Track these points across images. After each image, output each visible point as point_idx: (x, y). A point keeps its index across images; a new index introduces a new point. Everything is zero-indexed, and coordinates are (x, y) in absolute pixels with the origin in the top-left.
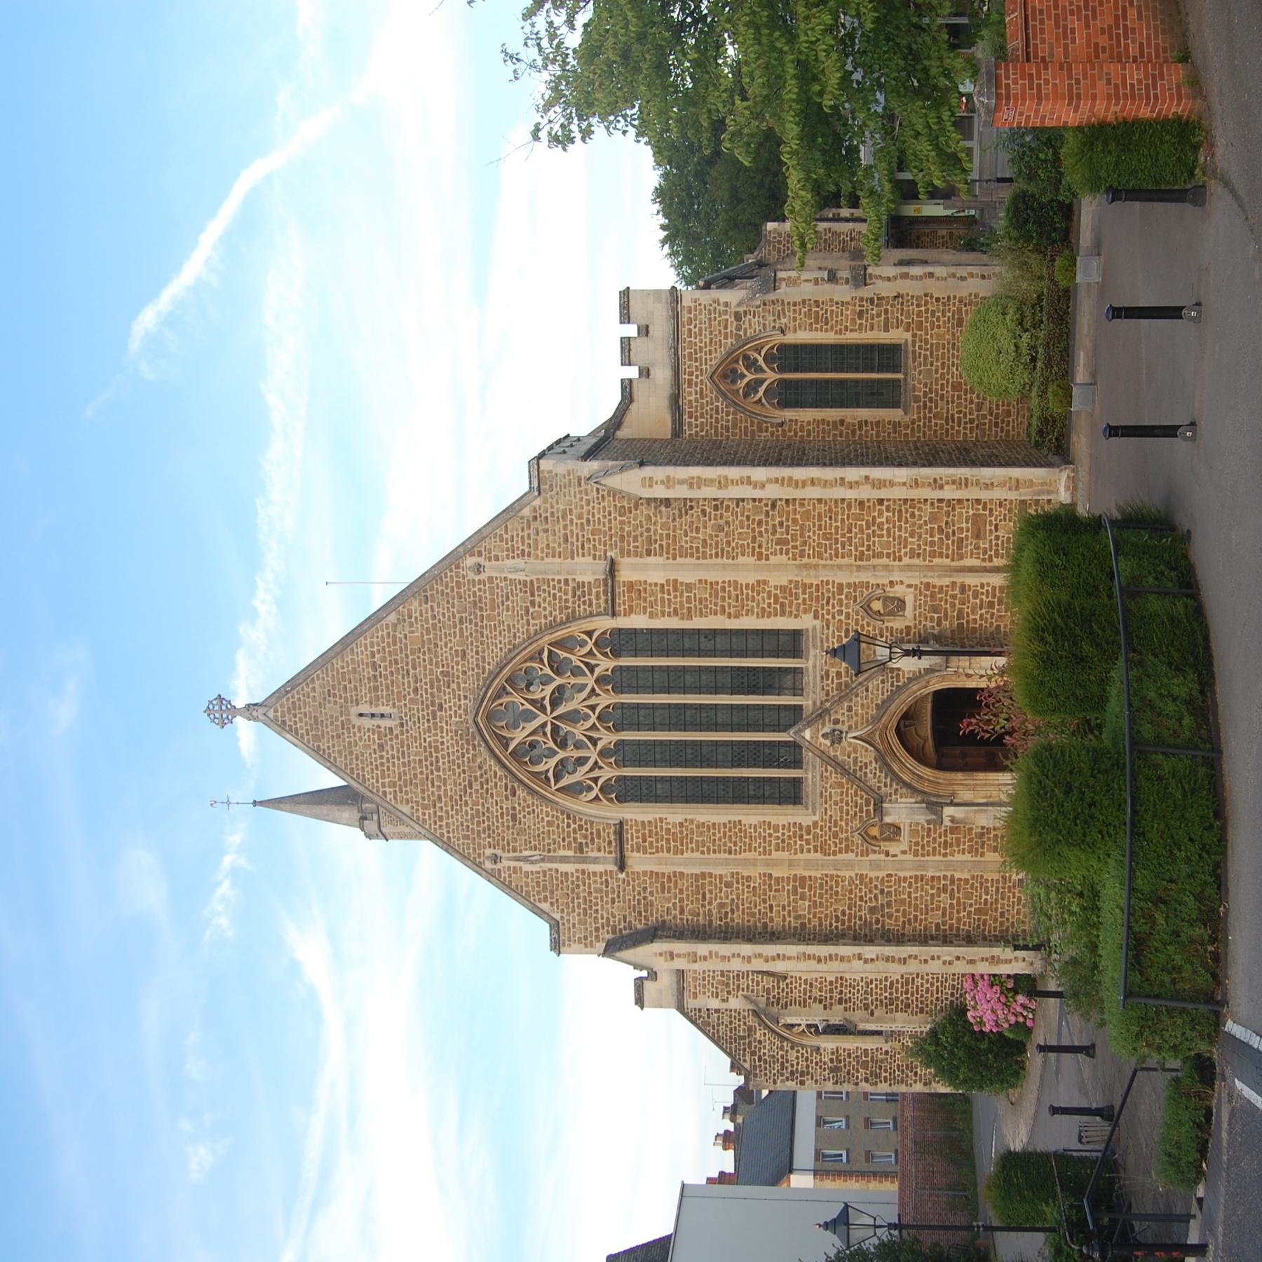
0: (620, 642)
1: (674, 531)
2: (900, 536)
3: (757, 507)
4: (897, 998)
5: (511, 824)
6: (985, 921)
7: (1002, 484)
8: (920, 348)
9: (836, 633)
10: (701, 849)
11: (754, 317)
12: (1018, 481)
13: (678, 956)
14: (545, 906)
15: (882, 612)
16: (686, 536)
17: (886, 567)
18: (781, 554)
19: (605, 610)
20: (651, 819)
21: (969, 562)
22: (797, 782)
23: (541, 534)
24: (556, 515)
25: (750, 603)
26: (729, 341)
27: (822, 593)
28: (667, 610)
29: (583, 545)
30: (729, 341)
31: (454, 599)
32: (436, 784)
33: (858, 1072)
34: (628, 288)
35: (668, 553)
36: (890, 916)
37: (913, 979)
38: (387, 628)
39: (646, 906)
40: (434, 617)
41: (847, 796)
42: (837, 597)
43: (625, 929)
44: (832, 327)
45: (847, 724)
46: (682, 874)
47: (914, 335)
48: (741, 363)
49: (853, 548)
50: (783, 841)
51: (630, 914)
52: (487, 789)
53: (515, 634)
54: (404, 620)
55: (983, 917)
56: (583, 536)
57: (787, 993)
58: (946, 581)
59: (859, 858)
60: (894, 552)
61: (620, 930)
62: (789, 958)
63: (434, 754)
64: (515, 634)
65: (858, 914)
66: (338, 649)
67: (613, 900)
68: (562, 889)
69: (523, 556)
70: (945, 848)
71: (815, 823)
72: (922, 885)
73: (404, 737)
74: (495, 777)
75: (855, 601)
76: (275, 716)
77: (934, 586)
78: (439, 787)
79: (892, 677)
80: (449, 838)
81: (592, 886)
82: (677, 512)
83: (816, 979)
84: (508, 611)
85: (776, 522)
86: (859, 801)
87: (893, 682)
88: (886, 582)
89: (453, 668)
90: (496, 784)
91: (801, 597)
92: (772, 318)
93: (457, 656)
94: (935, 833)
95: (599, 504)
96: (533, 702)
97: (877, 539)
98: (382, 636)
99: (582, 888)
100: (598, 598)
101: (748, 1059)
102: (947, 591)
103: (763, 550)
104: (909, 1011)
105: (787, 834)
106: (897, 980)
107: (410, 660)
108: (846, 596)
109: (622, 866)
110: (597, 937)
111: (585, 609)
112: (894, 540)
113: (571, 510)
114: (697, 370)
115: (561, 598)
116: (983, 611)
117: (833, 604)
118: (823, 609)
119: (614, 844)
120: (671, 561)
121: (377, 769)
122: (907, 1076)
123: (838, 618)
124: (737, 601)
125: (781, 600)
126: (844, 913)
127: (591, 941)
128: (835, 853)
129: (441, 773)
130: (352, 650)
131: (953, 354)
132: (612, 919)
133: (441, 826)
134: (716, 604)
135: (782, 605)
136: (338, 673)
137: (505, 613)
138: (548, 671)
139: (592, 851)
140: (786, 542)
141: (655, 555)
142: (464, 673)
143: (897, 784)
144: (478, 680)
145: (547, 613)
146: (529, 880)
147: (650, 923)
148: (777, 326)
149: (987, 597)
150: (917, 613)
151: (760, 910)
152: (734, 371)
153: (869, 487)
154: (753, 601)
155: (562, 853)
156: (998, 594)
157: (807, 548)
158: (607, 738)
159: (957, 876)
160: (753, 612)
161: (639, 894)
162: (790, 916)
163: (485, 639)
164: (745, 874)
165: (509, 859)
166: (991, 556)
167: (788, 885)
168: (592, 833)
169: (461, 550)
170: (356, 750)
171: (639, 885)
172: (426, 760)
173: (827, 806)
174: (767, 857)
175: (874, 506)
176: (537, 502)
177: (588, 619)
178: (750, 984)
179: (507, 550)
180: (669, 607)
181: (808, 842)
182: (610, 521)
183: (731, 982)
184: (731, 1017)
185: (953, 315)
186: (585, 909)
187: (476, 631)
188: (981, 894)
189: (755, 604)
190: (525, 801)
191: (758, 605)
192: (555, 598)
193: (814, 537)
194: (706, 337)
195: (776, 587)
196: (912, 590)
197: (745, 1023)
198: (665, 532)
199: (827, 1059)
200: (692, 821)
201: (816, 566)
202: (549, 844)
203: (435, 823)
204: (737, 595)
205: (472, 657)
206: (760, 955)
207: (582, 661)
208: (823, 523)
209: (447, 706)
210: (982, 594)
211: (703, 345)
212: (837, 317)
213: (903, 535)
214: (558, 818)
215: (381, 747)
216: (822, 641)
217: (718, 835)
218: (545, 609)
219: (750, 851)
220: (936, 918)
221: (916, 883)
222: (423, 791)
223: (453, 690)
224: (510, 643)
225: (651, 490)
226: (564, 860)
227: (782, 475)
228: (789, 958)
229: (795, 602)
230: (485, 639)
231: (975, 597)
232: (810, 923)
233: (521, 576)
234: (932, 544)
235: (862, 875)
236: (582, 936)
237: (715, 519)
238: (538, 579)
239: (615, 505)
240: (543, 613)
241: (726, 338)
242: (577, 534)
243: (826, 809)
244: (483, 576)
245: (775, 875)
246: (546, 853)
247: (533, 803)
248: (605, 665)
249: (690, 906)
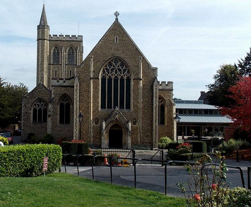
0: (129, 80)
13: (77, 88)
14: (83, 65)
21: (142, 134)
22: (105, 108)
58: (139, 131)
138: (124, 68)
140: (145, 107)
158: (113, 77)
234: (144, 129)
248: (125, 78)
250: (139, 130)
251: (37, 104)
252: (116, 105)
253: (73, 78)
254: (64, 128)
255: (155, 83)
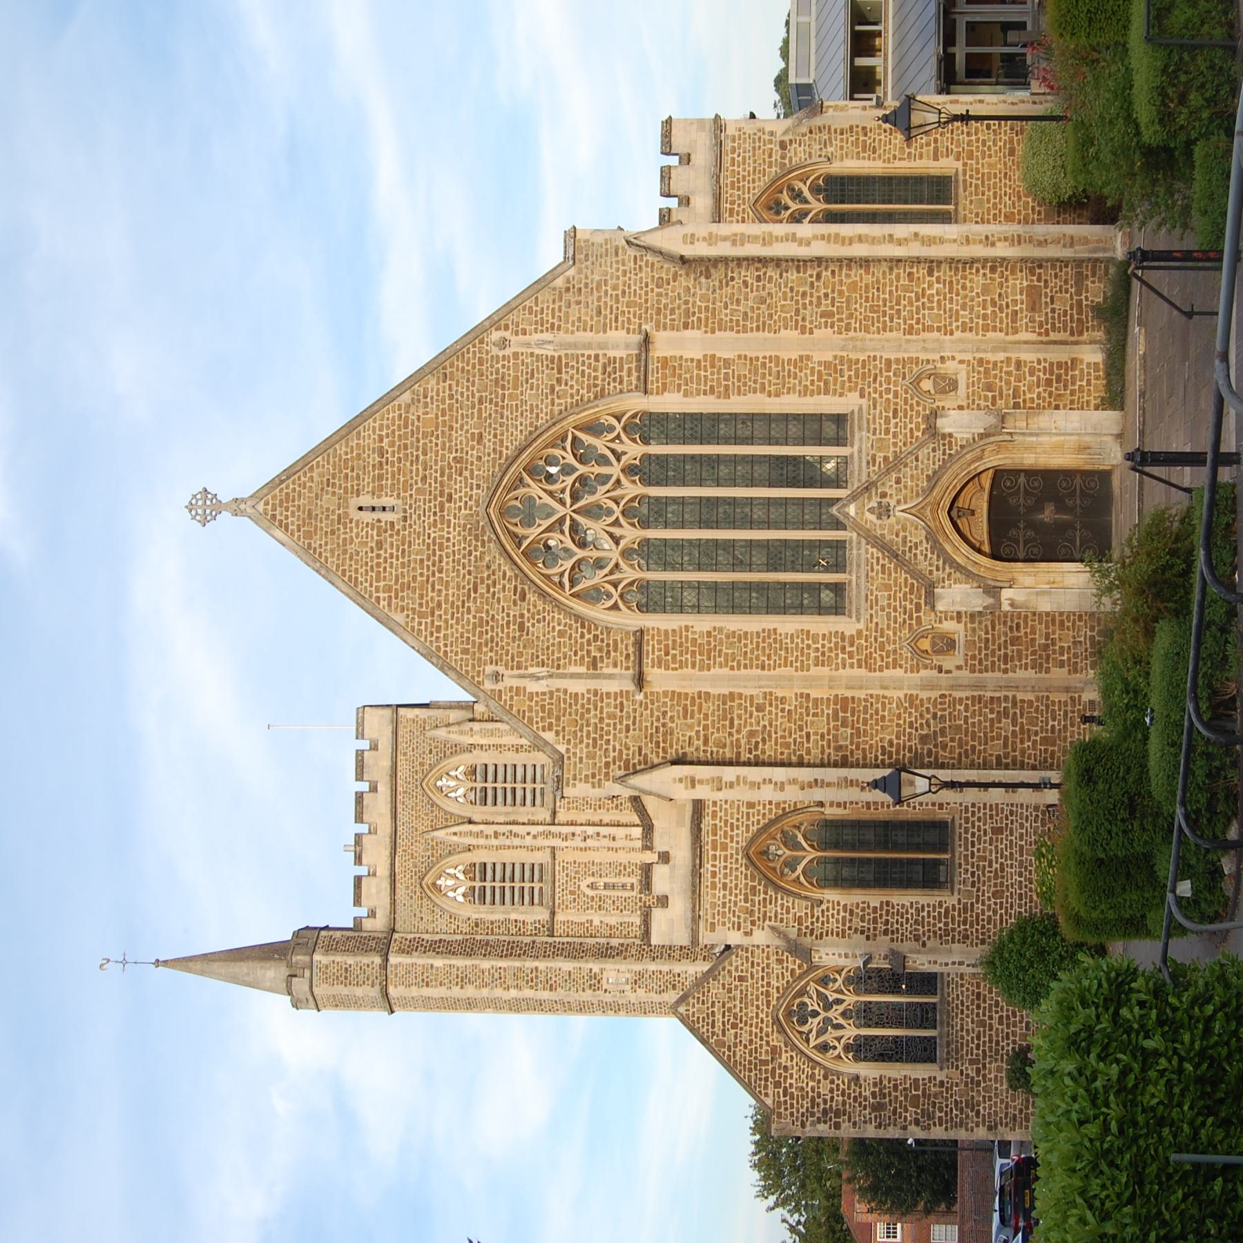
1: (714, 304)
2: (951, 309)
3: (801, 278)
4: (953, 930)
5: (517, 634)
6: (1053, 753)
7: (1056, 241)
8: (971, 177)
9: (884, 414)
10: (730, 664)
11: (800, 146)
12: (1072, 238)
13: (701, 782)
14: (549, 736)
15: (933, 392)
16: (726, 308)
17: (938, 340)
18: (826, 327)
19: (636, 387)
20: (676, 627)
21: (1024, 336)
22: (838, 589)
23: (573, 306)
24: (590, 286)
25: (791, 380)
26: (774, 169)
27: (869, 370)
28: (703, 388)
29: (617, 318)
30: (774, 169)
31: (474, 376)
32: (437, 587)
33: (906, 1111)
34: (670, 117)
35: (706, 326)
36: (944, 747)
37: (972, 904)
38: (399, 409)
39: (665, 734)
40: (451, 397)
41: (895, 601)
42: (885, 374)
43: (640, 764)
44: (880, 156)
45: (895, 498)
46: (707, 694)
47: (965, 164)
48: (785, 192)
49: (901, 321)
50: (823, 654)
51: (646, 745)
52: (494, 593)
53: (538, 414)
54: (419, 401)
55: (1050, 748)
56: (618, 308)
57: (823, 923)
58: (1001, 356)
59: (909, 674)
60: (945, 325)
61: (634, 764)
62: (829, 785)
63: (438, 553)
64: (538, 414)
65: (908, 744)
66: (343, 433)
67: (628, 726)
68: (570, 714)
69: (552, 328)
70: (1006, 663)
71: (859, 632)
72: (980, 708)
73: (407, 533)
74: (504, 579)
75: (904, 378)
76: (265, 509)
77: (988, 362)
78: (440, 591)
79: (944, 445)
80: (446, 652)
81: (605, 710)
82: (717, 284)
83: (858, 904)
84: (532, 389)
85: (821, 294)
86: (908, 607)
87: (945, 450)
88: (937, 357)
89: (467, 453)
90: (504, 587)
91: (847, 374)
92: (818, 147)
93: (473, 440)
94: (994, 645)
95: (636, 274)
96: (551, 494)
97: (927, 312)
98: (393, 417)
99: (593, 712)
100: (629, 375)
101: (770, 1092)
102: (1002, 367)
103: (807, 324)
104: (969, 942)
105: (828, 645)
106: (953, 905)
107: (421, 444)
108: (895, 374)
109: (640, 681)
110: (607, 774)
111: (615, 387)
112: (945, 313)
113: (606, 281)
114: (739, 199)
115: (589, 376)
116: (1041, 389)
117: (881, 382)
118: (869, 387)
119: (632, 658)
120: (709, 334)
121: (372, 571)
122: (967, 1116)
123: (885, 396)
124: (778, 378)
125: (825, 377)
126: (891, 743)
127: (600, 780)
128: (881, 670)
129: (444, 575)
130: (359, 433)
131: (1005, 184)
132: (625, 752)
133: (438, 638)
134: (755, 381)
135: (826, 383)
136: (340, 461)
137: (528, 391)
139: (607, 667)
140: (831, 315)
141: (693, 328)
142: (479, 458)
143: (951, 568)
144: (494, 466)
145: (574, 391)
146: (533, 703)
147: (668, 757)
148: (823, 154)
149: (1045, 374)
150: (970, 390)
151: (795, 740)
152: (778, 203)
153: (918, 244)
154: (795, 378)
155: (573, 669)
156: (1056, 371)
157: (853, 321)
159: (1020, 696)
160: (794, 388)
161: (658, 720)
162: (829, 747)
163: (505, 420)
164: (780, 695)
165: (513, 677)
166: (1047, 329)
167: (828, 709)
168: (608, 645)
169: (487, 323)
170: (351, 548)
171: (658, 709)
172: (428, 560)
173: (873, 612)
174: (805, 673)
175: (924, 277)
176: (571, 272)
177: (619, 396)
178: (779, 911)
179: (536, 323)
180: (706, 386)
181: (851, 656)
182: (646, 293)
183: (756, 909)
184: (751, 1035)
185: (1005, 144)
186: (595, 739)
187: (496, 411)
188: (1047, 718)
189: (797, 382)
190: (535, 606)
191: (800, 383)
192: (583, 376)
193: (860, 309)
194: (749, 166)
195: (820, 363)
196: (964, 366)
197: (768, 1043)
198: (703, 305)
199: (868, 1093)
200: (721, 630)
201: (863, 340)
202: (559, 659)
203: (432, 634)
204: (779, 372)
205: (489, 440)
206: (794, 781)
207: (608, 448)
208: (871, 295)
209: (457, 496)
210: (1039, 370)
211: (746, 174)
212: (885, 146)
213: (955, 308)
214: (570, 627)
215: (380, 545)
216: (868, 420)
217: (750, 646)
218: (572, 387)
219: (786, 666)
220: (996, 748)
221: (973, 705)
222: (421, 596)
223: (466, 478)
224: (531, 424)
225: (692, 246)
226: (573, 676)
227: (829, 231)
228: (829, 785)
229: (840, 379)
230: (505, 420)
231: (1032, 373)
232: (852, 757)
233: (549, 351)
234: (985, 317)
235: (911, 695)
236: (589, 773)
237: (757, 291)
238: (566, 355)
239: (653, 276)
240: (570, 391)
241: (770, 166)
242: (611, 307)
243: (871, 615)
244: (508, 352)
245: (814, 695)
246: (554, 670)
247: (544, 608)
248: (634, 450)
249: (716, 735)
250: (995, 350)
251: (821, 1032)
252: (820, 514)
253: (636, 802)
254: (984, 859)
255: (672, 241)
